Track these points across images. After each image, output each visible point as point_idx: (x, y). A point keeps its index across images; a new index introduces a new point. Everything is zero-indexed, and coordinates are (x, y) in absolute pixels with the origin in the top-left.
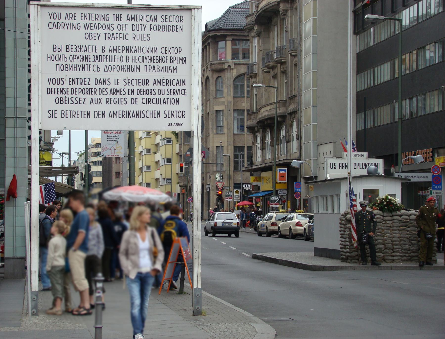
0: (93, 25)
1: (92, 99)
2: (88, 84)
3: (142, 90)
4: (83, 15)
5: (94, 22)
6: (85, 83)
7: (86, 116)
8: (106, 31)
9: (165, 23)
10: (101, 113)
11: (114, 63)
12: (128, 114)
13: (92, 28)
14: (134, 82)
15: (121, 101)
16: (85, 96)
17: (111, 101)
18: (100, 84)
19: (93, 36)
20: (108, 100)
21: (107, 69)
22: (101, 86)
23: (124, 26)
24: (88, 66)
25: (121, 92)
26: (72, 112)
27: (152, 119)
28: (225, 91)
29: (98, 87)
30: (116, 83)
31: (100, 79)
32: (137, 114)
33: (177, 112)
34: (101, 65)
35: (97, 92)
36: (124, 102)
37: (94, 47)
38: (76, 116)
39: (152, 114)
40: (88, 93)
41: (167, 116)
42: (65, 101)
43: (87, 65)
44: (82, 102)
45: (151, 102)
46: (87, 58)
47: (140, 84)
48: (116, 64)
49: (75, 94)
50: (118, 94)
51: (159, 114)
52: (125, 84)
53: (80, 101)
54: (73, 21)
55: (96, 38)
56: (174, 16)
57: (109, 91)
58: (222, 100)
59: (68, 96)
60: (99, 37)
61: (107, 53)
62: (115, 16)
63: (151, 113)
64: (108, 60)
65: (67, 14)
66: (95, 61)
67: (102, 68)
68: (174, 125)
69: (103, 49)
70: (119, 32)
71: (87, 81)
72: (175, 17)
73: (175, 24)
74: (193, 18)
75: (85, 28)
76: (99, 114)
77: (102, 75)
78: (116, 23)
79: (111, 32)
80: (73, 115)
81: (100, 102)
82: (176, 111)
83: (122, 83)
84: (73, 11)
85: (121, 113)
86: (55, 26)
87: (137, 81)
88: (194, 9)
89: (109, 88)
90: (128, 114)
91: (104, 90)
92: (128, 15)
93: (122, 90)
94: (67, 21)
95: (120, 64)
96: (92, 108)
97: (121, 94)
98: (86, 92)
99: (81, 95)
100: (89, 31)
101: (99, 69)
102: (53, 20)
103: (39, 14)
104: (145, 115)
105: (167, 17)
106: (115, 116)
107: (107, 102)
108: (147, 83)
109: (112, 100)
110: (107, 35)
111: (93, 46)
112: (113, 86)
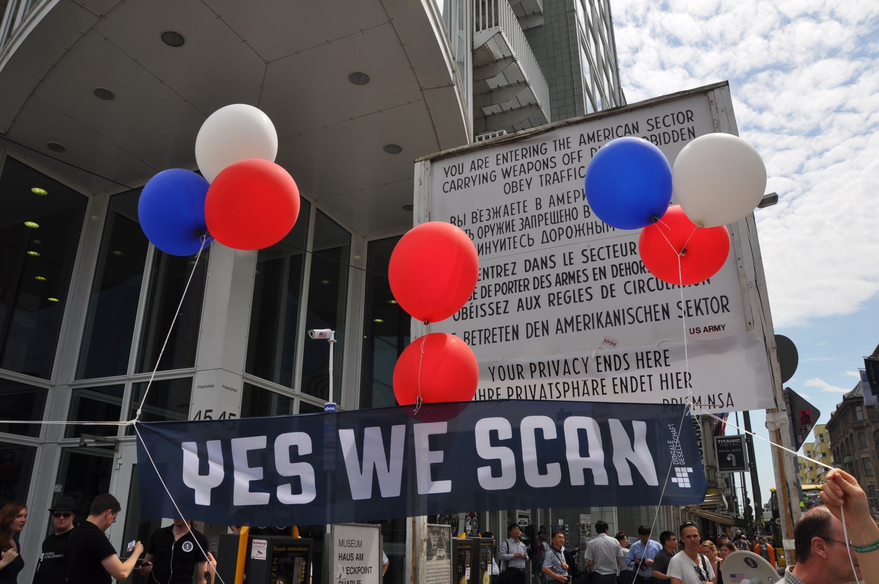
0: (518, 168)
1: (520, 300)
2: (513, 274)
3: (623, 267)
4: (500, 157)
5: (519, 163)
6: (507, 273)
7: (510, 336)
8: (542, 172)
9: (656, 132)
10: (539, 325)
11: (560, 225)
12: (597, 320)
13: (517, 173)
14: (604, 253)
15: (580, 295)
16: (505, 298)
17: (559, 298)
18: (536, 268)
19: (518, 186)
20: (552, 296)
21: (547, 238)
22: (537, 273)
23: (575, 155)
24: (512, 240)
25: (578, 277)
26: (483, 333)
27: (650, 325)
28: (868, 443)
29: (530, 275)
30: (567, 262)
31: (535, 260)
32: (617, 318)
33: (709, 301)
34: (536, 233)
35: (531, 286)
36: (586, 296)
37: (521, 205)
38: (490, 339)
39: (650, 313)
40: (513, 290)
42: (471, 312)
43: (509, 238)
44: (501, 311)
45: (646, 288)
46: (509, 226)
47: (617, 254)
48: (564, 225)
49: (489, 296)
50: (572, 282)
51: (666, 312)
52: (585, 259)
53: (498, 308)
54: (483, 171)
55: (525, 187)
56: (673, 115)
57: (553, 279)
58: (866, 450)
59: (475, 303)
60: (529, 185)
61: (546, 209)
62: (557, 143)
63: (648, 311)
64: (548, 222)
65: (473, 162)
66: (524, 227)
67: (538, 239)
68: (705, 330)
69: (538, 204)
70: (566, 168)
71: (510, 267)
72: (675, 116)
73: (677, 127)
74: (713, 107)
75: (505, 177)
76: (536, 329)
77: (539, 251)
78: (559, 155)
79: (551, 171)
80: (486, 338)
81: (537, 303)
82: (706, 299)
83: (578, 259)
84: (482, 155)
85: (580, 319)
86: (455, 186)
87: (611, 249)
88: (712, 90)
89: (553, 273)
90: (597, 320)
91: (544, 279)
92: (582, 135)
93: (580, 273)
94: (474, 173)
95: (572, 223)
96: (520, 318)
97: (579, 282)
98: (508, 288)
99: (500, 297)
100: (510, 180)
101: (531, 241)
102: (450, 178)
103: (428, 173)
104: (635, 319)
105: (660, 120)
106: (569, 329)
107: (550, 302)
108: (631, 250)
109: (560, 295)
110: (544, 178)
111: (518, 203)
112: (560, 269)
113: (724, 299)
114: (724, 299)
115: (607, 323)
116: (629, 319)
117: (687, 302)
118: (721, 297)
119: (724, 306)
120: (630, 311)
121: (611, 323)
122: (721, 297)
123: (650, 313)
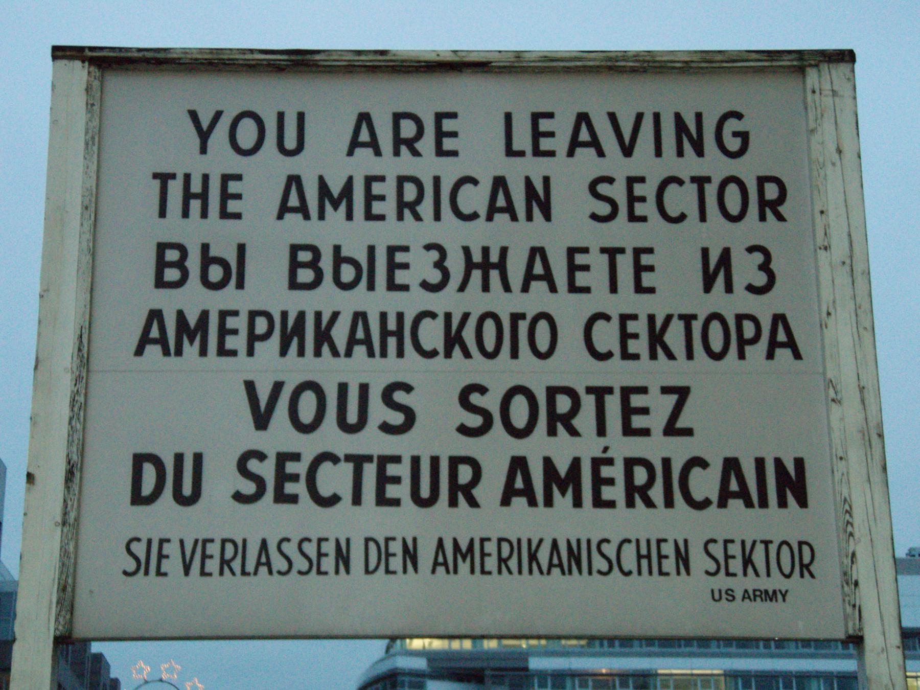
10: (396, 547)
32: (572, 558)
39: (650, 557)
41: (721, 567)
51: (683, 559)
63: (644, 551)
76: (388, 555)
82: (767, 543)
104: (614, 565)
106: (464, 567)
113: (806, 549)
114: (806, 550)
115: (551, 565)
116: (600, 563)
117: (726, 542)
118: (801, 543)
119: (802, 565)
120: (605, 547)
121: (560, 565)
122: (801, 543)
123: (648, 557)
